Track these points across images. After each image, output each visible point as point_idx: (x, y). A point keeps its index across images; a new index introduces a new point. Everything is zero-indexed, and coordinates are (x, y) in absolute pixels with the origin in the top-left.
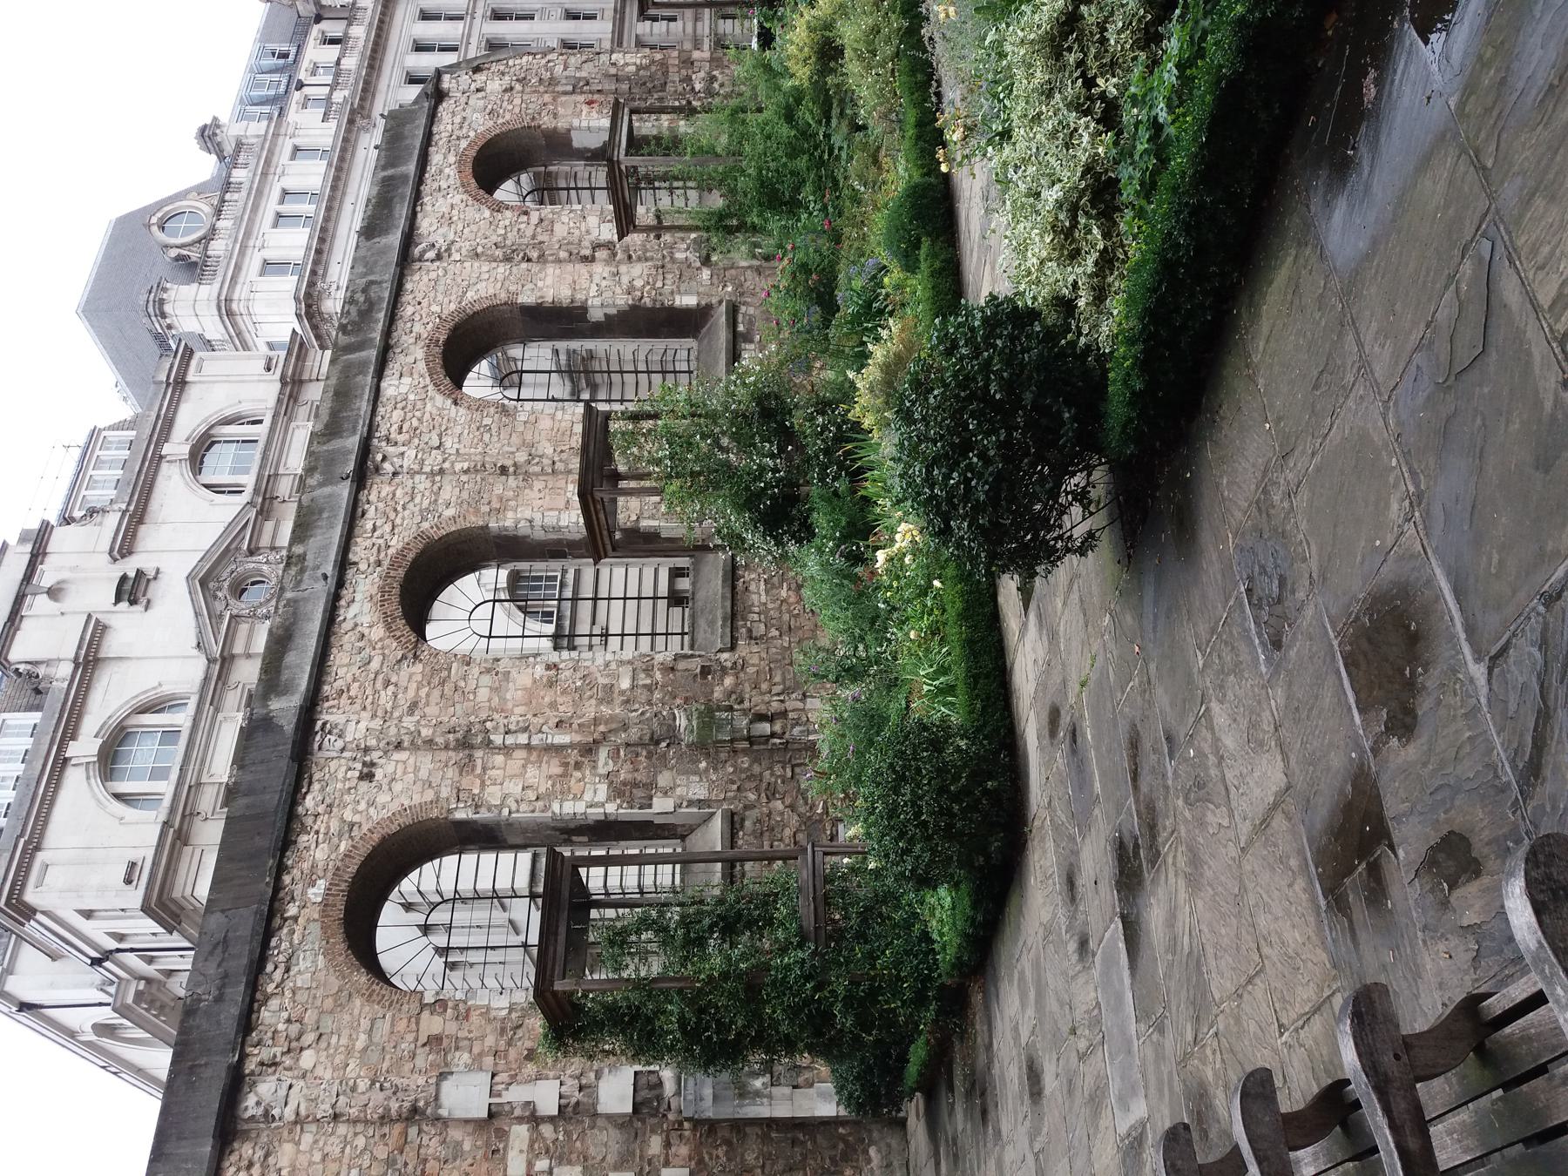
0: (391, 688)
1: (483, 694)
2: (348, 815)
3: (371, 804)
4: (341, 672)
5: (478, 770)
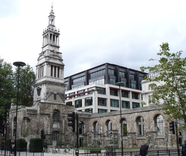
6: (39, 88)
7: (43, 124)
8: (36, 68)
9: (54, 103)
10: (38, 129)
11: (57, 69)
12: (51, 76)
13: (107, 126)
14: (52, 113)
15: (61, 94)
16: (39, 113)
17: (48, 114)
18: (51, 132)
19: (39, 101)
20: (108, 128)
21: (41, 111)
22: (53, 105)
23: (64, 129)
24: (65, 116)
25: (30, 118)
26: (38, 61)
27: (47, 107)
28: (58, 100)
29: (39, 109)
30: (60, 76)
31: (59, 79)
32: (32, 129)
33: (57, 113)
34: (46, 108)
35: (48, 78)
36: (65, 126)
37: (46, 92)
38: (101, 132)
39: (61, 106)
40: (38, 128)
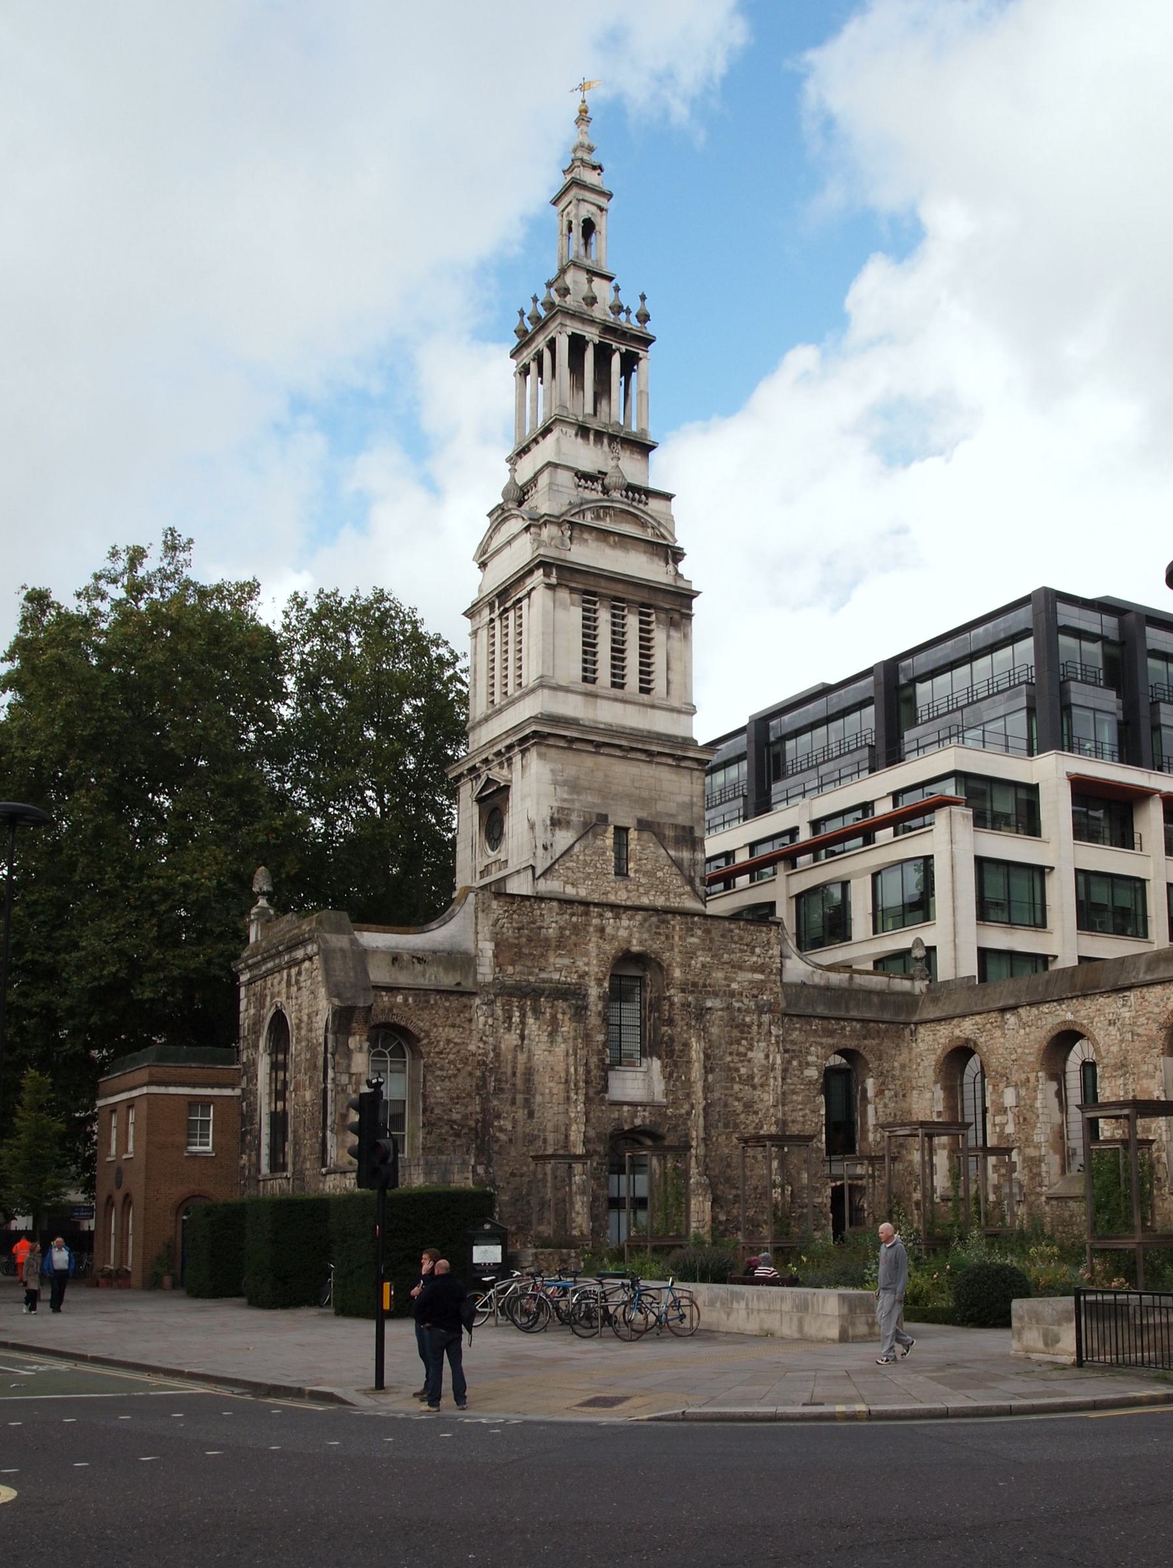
0: (1146, 1022)
1: (1144, 1068)
2: (1096, 1019)
3: (1100, 1028)
4: (1152, 995)
5: (1114, 1074)
6: (489, 782)
7: (529, 1072)
8: (467, 625)
9: (612, 898)
10: (484, 1110)
11: (632, 622)
12: (585, 679)
13: (1054, 1086)
14: (599, 982)
15: (675, 826)
16: (489, 978)
18: (592, 1133)
19: (498, 891)
20: (1061, 1095)
21: (510, 969)
22: (609, 914)
24: (709, 1004)
25: (410, 1027)
26: (483, 565)
28: (650, 874)
29: (490, 954)
30: (659, 684)
31: (653, 707)
33: (640, 978)
34: (547, 939)
35: (561, 694)
36: (707, 1089)
37: (546, 813)
38: (1010, 1129)
40: (485, 1101)
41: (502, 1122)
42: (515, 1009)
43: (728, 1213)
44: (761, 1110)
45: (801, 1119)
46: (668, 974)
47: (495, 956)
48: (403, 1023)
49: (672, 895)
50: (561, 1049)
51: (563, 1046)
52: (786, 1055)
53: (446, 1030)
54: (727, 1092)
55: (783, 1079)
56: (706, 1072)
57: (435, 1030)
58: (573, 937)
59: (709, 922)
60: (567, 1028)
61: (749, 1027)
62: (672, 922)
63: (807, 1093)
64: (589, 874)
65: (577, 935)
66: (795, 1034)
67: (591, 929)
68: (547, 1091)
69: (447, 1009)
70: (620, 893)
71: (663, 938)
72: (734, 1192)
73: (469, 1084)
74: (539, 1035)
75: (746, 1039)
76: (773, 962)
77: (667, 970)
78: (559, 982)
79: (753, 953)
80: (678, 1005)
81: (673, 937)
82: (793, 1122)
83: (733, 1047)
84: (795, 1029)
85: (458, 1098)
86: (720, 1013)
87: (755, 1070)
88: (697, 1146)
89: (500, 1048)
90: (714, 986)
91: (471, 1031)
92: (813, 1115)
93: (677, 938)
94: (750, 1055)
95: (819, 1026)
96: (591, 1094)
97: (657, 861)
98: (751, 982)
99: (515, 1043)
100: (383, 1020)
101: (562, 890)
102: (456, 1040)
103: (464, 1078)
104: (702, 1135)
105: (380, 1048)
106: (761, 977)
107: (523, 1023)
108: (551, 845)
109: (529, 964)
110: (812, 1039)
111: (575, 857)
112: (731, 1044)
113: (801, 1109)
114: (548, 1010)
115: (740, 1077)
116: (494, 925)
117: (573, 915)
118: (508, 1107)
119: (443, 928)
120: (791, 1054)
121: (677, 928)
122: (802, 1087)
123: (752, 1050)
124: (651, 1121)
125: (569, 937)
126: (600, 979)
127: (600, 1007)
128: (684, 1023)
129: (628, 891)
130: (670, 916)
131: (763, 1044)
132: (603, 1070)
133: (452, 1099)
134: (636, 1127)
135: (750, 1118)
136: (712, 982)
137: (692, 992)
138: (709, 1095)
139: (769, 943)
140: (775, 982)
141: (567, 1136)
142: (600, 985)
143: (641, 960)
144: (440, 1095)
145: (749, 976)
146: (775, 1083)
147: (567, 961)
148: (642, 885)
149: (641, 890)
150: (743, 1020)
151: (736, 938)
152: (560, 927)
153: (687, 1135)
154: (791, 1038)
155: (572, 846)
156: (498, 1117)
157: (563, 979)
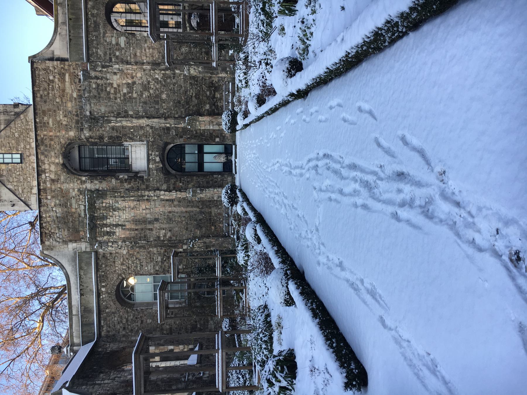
7: (136, 221)
17: (92, 207)
18: (165, 187)
22: (43, 176)
23: (149, 122)
24: (88, 113)
25: (117, 283)
27: (59, 210)
29: (74, 245)
32: (157, 268)
39: (42, 133)
40: (151, 246)
41: (161, 235)
42: (103, 230)
43: (205, 104)
44: (147, 79)
45: (151, 50)
46: (73, 140)
47: (76, 241)
48: (115, 288)
49: (28, 127)
50: (121, 204)
51: (120, 203)
52: (113, 60)
53: (117, 265)
54: (138, 101)
55: (128, 63)
56: (128, 117)
57: (117, 271)
58: (59, 198)
59: (37, 111)
60: (109, 201)
61: (98, 85)
62: (42, 136)
63: (134, 45)
64: (24, 179)
65: (58, 196)
66: (100, 52)
67: (53, 187)
68: (144, 211)
69: (106, 266)
70: (32, 161)
71: (52, 143)
72: (194, 99)
73: (144, 253)
74: (115, 217)
75: (106, 88)
76: (57, 66)
77: (71, 140)
78: (85, 206)
79: (53, 81)
80: (91, 133)
81: (51, 136)
82: (153, 56)
83: (112, 97)
84: (97, 52)
85: (150, 258)
86: (92, 106)
87: (124, 82)
88: (169, 123)
89: (124, 238)
90: (76, 109)
91: (116, 253)
92: (148, 41)
93: (51, 134)
94: (115, 85)
95: (94, 33)
96: (144, 187)
97: (9, 137)
98: (71, 84)
99: (120, 229)
100: (115, 297)
101: (35, 195)
102: (122, 260)
103: (140, 255)
104: (163, 121)
105: (130, 289)
106: (67, 75)
107: (109, 226)
108: (11, 202)
109: (77, 223)
110: (102, 39)
111: (16, 188)
112: (110, 98)
113: (145, 50)
114: (101, 212)
115: (129, 93)
116: (59, 242)
117: (47, 199)
118: (154, 232)
119: (65, 266)
120: (112, 56)
121: (45, 133)
122: (132, 49)
123: (112, 84)
124: (157, 151)
125: (60, 201)
126: (81, 182)
127: (96, 182)
128: (100, 130)
129: (30, 155)
130: (39, 138)
131: (108, 76)
132: (131, 180)
133: (151, 261)
134: (161, 160)
135: (152, 86)
136: (74, 110)
137: (82, 123)
138: (140, 114)
139: (44, 70)
140: (69, 66)
141: (167, 200)
142: (85, 182)
143: (67, 154)
144: (149, 267)
145: (67, 84)
146: (129, 69)
147: (73, 201)
148: (25, 146)
149: (28, 147)
150: (95, 89)
151: (46, 93)
152: (55, 206)
153: (164, 129)
154: (102, 55)
155: (9, 189)
156: (159, 237)
157: (83, 203)
